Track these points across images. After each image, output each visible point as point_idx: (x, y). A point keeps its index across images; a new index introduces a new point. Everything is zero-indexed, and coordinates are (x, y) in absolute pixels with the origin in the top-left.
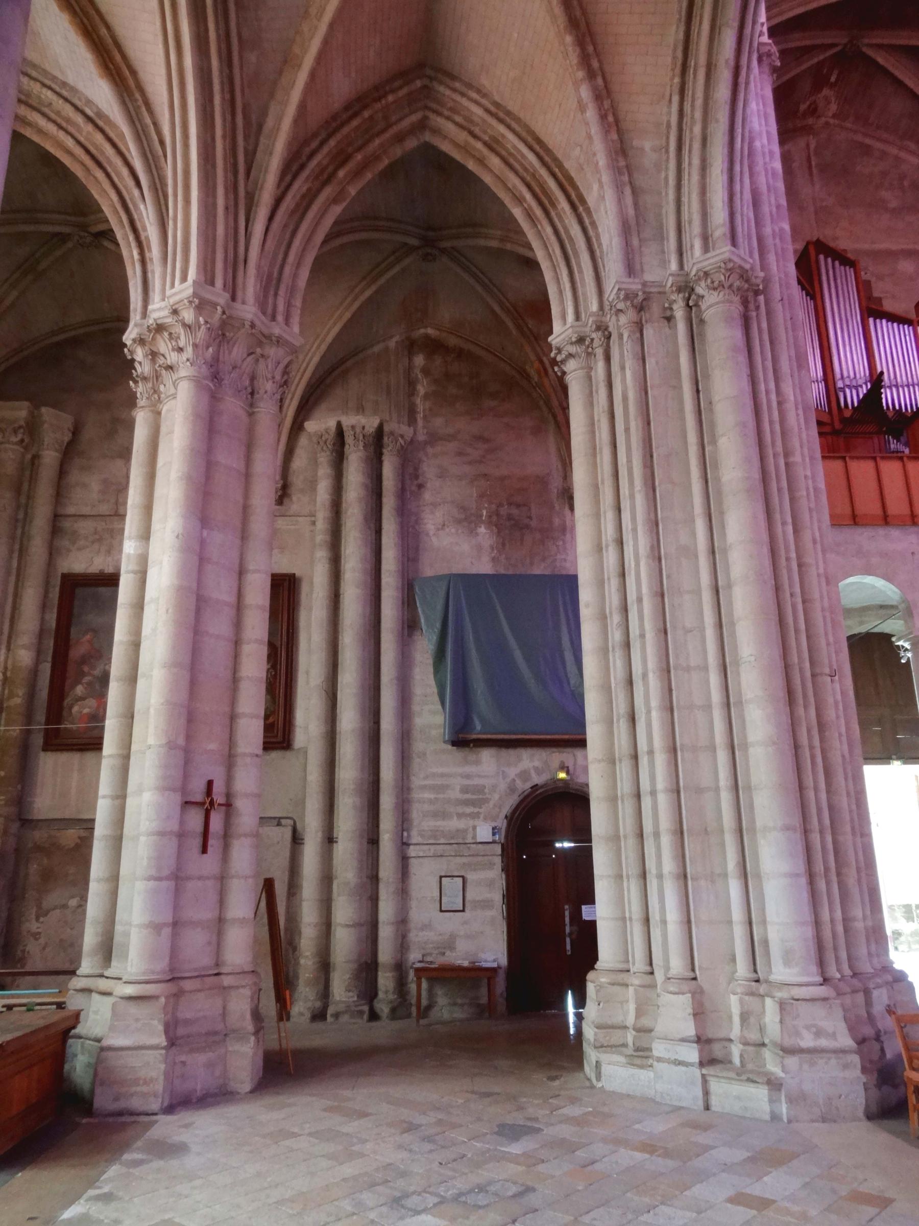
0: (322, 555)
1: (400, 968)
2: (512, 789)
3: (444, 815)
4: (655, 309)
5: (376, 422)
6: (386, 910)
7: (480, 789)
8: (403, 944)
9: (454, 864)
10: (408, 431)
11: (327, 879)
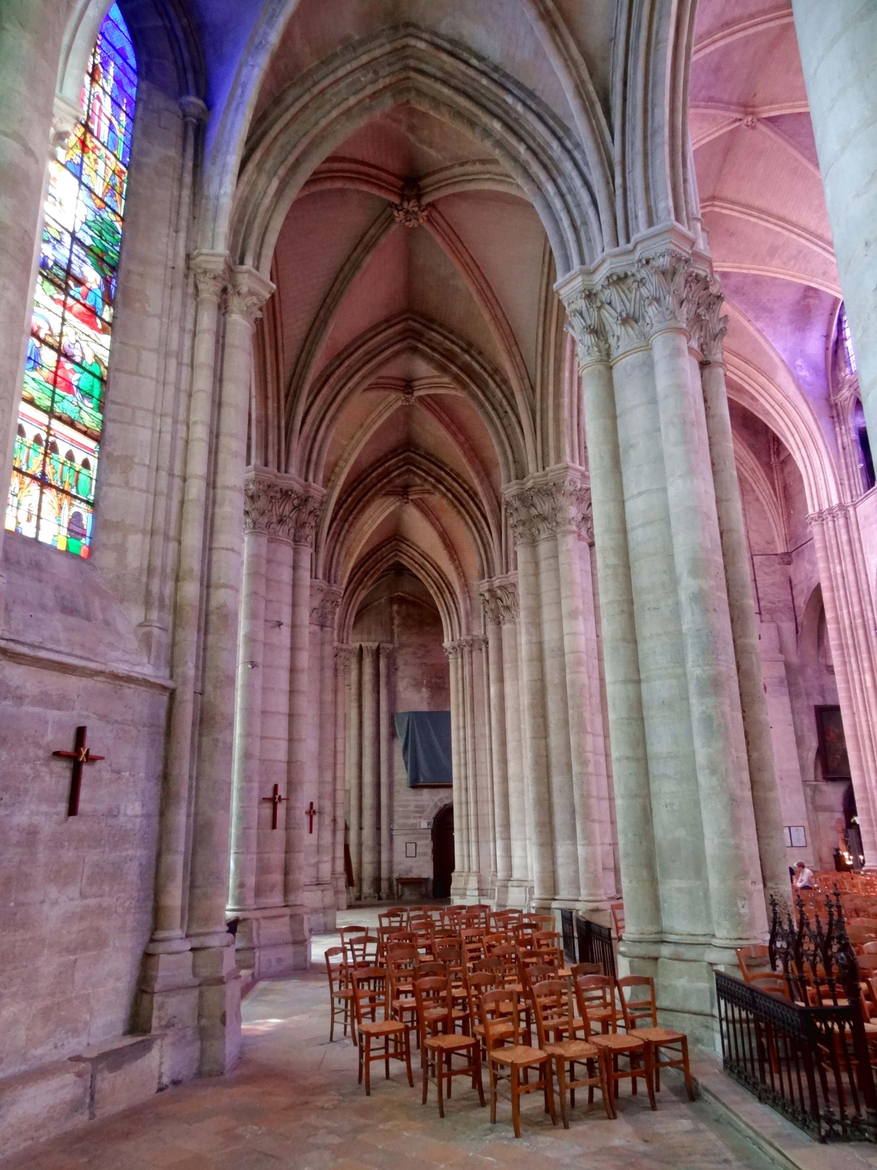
0: (354, 705)
1: (390, 880)
2: (436, 806)
3: (408, 818)
4: (476, 646)
5: (376, 644)
6: (384, 857)
7: (422, 806)
8: (391, 871)
9: (411, 838)
10: (390, 646)
11: (360, 845)
